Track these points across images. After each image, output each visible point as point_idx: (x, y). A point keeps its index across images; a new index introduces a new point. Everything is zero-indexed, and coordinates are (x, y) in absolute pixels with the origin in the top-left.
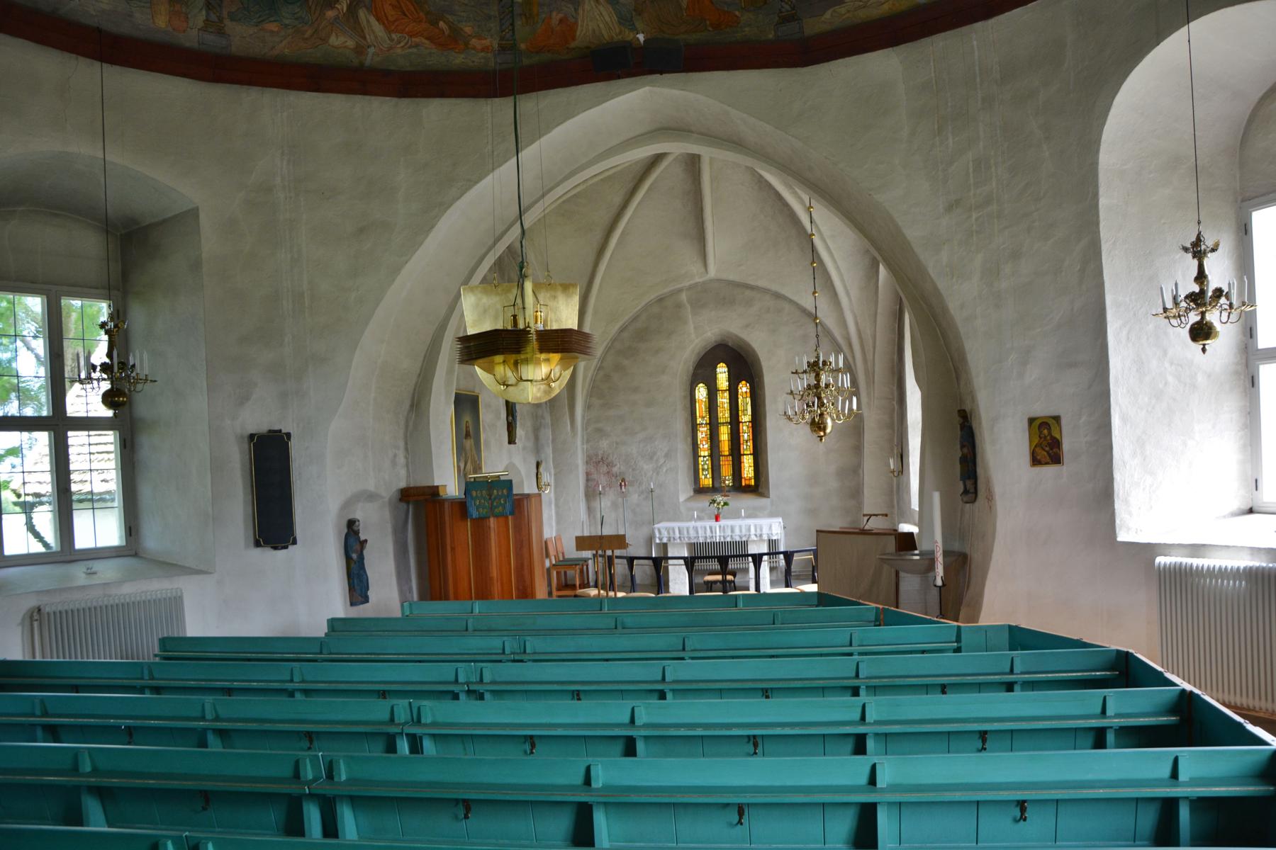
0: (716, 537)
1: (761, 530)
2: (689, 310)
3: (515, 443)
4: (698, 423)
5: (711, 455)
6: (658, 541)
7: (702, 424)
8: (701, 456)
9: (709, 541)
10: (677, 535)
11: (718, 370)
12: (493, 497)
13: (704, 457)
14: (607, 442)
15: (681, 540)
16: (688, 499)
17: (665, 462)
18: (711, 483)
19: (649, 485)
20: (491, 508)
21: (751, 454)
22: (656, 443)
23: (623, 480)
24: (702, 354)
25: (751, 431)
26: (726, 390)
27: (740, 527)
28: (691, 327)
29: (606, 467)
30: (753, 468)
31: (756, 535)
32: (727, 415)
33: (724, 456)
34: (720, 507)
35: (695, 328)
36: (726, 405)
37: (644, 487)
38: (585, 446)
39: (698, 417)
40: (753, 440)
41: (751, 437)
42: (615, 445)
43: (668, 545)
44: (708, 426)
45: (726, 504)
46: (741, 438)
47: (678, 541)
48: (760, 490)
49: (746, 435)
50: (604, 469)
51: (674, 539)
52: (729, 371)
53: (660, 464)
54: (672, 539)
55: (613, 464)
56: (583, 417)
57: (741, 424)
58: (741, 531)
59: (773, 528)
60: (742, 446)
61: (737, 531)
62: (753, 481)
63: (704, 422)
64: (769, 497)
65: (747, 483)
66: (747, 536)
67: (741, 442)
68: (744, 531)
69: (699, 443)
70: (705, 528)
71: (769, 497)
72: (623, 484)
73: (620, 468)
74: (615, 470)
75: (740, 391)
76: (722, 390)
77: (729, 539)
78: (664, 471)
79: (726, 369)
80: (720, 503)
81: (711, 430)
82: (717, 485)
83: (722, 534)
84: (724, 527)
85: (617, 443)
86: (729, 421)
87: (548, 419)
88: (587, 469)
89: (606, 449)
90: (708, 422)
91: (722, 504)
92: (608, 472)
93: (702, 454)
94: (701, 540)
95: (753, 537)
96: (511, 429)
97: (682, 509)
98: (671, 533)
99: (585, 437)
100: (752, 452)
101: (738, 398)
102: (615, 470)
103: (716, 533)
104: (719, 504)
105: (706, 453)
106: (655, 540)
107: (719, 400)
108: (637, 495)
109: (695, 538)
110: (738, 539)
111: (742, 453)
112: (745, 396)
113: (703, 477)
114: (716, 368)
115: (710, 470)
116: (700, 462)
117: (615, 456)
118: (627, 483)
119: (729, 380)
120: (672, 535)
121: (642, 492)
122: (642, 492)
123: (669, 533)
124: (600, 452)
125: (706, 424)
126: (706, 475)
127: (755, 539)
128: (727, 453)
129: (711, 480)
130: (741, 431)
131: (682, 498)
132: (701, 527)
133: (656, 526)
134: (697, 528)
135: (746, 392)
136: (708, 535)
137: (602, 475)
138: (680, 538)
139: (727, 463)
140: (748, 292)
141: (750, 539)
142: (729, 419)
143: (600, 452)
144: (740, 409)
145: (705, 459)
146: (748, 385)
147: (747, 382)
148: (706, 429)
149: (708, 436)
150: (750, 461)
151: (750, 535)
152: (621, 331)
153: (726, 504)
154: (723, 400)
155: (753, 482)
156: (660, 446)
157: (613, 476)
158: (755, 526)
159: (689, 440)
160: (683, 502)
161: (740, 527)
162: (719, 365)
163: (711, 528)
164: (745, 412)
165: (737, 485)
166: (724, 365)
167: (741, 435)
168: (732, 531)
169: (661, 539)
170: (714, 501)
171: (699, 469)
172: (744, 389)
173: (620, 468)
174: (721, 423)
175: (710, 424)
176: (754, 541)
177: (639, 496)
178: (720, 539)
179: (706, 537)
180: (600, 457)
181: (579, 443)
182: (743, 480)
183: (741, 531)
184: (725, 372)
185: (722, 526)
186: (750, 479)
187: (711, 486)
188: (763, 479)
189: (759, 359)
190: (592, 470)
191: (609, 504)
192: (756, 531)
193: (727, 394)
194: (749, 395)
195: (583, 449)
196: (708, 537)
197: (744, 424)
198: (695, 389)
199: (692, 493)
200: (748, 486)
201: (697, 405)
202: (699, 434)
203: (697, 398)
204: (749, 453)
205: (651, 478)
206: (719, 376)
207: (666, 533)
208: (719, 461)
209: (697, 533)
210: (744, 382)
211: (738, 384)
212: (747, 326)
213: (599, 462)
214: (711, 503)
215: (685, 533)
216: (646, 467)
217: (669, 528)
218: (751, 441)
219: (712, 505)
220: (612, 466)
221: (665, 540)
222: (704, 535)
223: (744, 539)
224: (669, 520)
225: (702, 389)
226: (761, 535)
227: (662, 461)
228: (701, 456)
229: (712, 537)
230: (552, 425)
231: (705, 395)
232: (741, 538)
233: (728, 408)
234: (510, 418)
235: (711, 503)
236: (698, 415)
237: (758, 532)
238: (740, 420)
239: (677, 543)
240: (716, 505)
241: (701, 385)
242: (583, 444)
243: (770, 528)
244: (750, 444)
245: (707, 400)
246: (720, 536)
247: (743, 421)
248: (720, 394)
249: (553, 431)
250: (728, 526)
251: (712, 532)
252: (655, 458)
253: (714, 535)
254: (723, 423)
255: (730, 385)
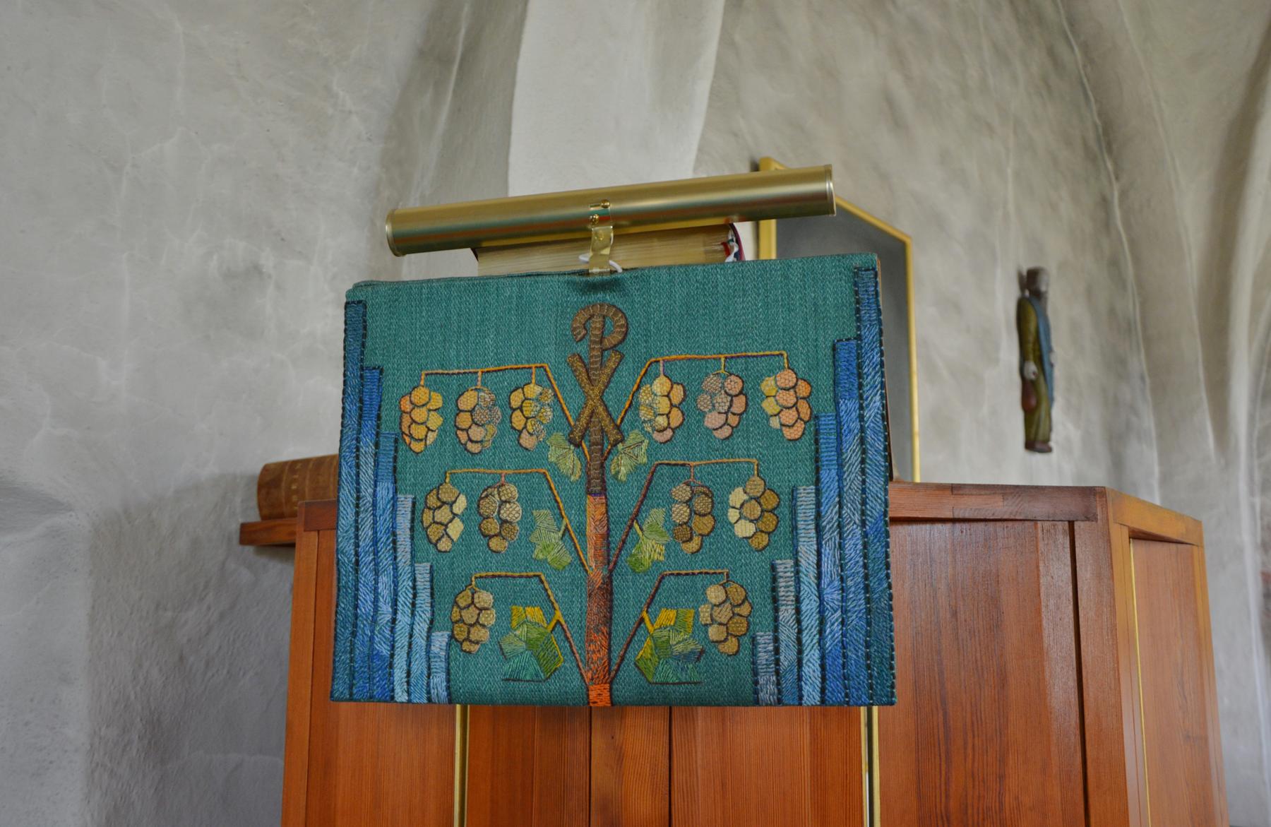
3: (1049, 450)
12: (622, 466)
20: (607, 590)
38: (1258, 501)
56: (1252, 418)
87: (1148, 421)
88: (1264, 564)
96: (1033, 402)
99: (1257, 476)
181: (1243, 487)
195: (1252, 507)
230: (1160, 437)
234: (1032, 367)
242: (1252, 493)
249: (1164, 456)
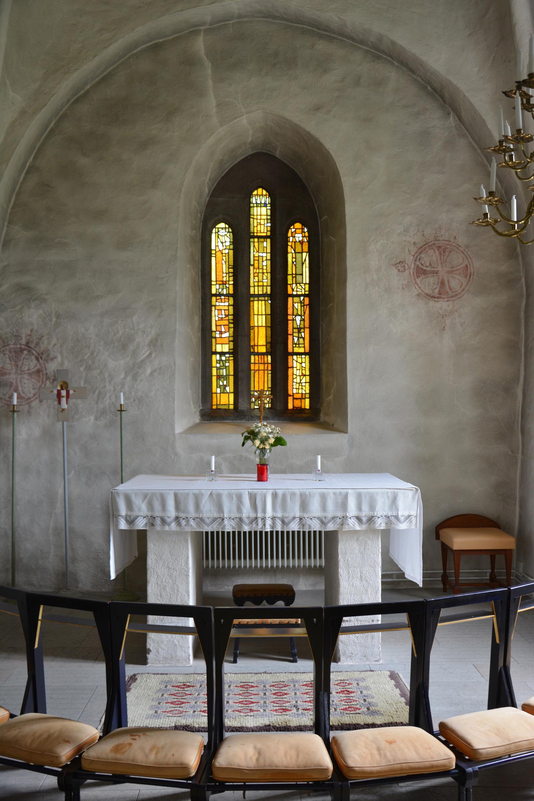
0: (264, 519)
1: (372, 507)
2: (209, 71)
4: (214, 291)
5: (234, 352)
6: (123, 525)
7: (220, 295)
8: (216, 353)
9: (246, 528)
10: (172, 512)
11: (253, 200)
13: (222, 354)
14: (41, 312)
15: (179, 524)
16: (192, 429)
17: (150, 354)
18: (232, 401)
19: (118, 398)
21: (305, 354)
22: (135, 318)
23: (65, 386)
24: (228, 166)
25: (307, 312)
26: (265, 237)
27: (324, 498)
28: (211, 102)
29: (35, 361)
30: (308, 379)
31: (359, 519)
32: (266, 280)
33: (258, 354)
34: (267, 447)
35: (218, 105)
36: (265, 263)
37: (107, 402)
39: (213, 283)
40: (310, 328)
41: (307, 324)
42: (54, 319)
43: (148, 534)
44: (231, 299)
45: (279, 441)
46: (290, 323)
47: (173, 526)
48: (323, 417)
49: (298, 318)
50: (32, 364)
51: (163, 521)
52: (272, 204)
53: (139, 360)
54: (158, 521)
55: (48, 356)
57: (290, 299)
58: (324, 508)
59: (401, 503)
60: (290, 337)
61: (315, 509)
62: (307, 401)
63: (225, 292)
64: (345, 431)
65: (297, 403)
66: (339, 521)
67: (290, 331)
68: (331, 510)
69: (214, 328)
70: (239, 498)
71: (345, 431)
72: (64, 393)
73: (62, 364)
74: (52, 367)
75: (291, 239)
76: (259, 237)
77: (294, 527)
78: (149, 371)
79: (268, 200)
80: (267, 438)
81: (235, 306)
82: (243, 406)
83: (279, 514)
84: (284, 495)
85: (58, 316)
86: (269, 292)
89: (35, 327)
90: (231, 292)
91: (272, 441)
92: (38, 371)
93: (219, 348)
94: (229, 527)
95: (353, 524)
97: (180, 447)
98: (157, 505)
100: (307, 350)
101: (287, 253)
102: (52, 367)
103: (264, 511)
104: (263, 442)
105: (226, 348)
106: (117, 524)
107: (253, 253)
108: (92, 418)
109: (215, 519)
110: (316, 526)
111: (290, 350)
112: (299, 249)
113: (219, 390)
114: (250, 195)
115: (231, 379)
116: (214, 364)
117: (54, 341)
118: (71, 392)
119: (273, 218)
120: (158, 513)
121: (103, 412)
122: (103, 412)
123: (150, 506)
124: (24, 333)
125: (228, 295)
126: (225, 386)
127: (358, 528)
128: (263, 350)
129: (232, 396)
130: (290, 311)
131: (180, 426)
132: (230, 496)
133: (121, 488)
134: (219, 496)
135: (301, 242)
136: (244, 516)
137: (26, 376)
138: (177, 518)
139: (262, 367)
140: (322, 46)
141: (346, 528)
142: (269, 288)
143: (24, 333)
144: (290, 272)
145: (223, 358)
146: (306, 230)
147: (304, 224)
148: (227, 304)
149: (231, 317)
150: (303, 365)
151: (345, 518)
152: (77, 101)
153: (279, 441)
154: (261, 254)
155: (307, 404)
156: (142, 326)
157: (48, 378)
158: (359, 497)
159: (197, 321)
160: (181, 434)
161: (324, 498)
162: (255, 193)
163: (253, 498)
164: (299, 278)
165: (279, 406)
166: (265, 192)
167: (290, 317)
168: (304, 506)
169: (131, 521)
170: (253, 435)
171: (211, 376)
172: (299, 237)
173: (62, 364)
174: (254, 296)
175: (234, 296)
176: (356, 532)
177: (96, 419)
178: (274, 525)
179: (241, 519)
180: (24, 341)
182: (290, 399)
183: (324, 508)
184: (265, 205)
185: (280, 493)
186: (302, 398)
187: (232, 407)
188: (329, 398)
189: (339, 172)
190: (8, 366)
191: (37, 432)
192: (359, 508)
193: (267, 244)
194: (306, 247)
196: (246, 521)
197: (296, 299)
198: (211, 233)
199: (197, 419)
200: (299, 411)
201: (213, 259)
202: (215, 313)
203: (213, 247)
204: (302, 350)
205: (123, 385)
206: (255, 211)
207: (144, 506)
208: (250, 363)
209: (220, 508)
210: (298, 225)
211: (289, 228)
212: (318, 108)
213: (22, 350)
214: (246, 438)
215: (191, 507)
216: (112, 364)
217: (153, 495)
218: (307, 331)
219: (249, 442)
220: (47, 361)
221: (141, 524)
222: (235, 514)
223: (331, 527)
224: (155, 471)
225: (222, 232)
226: (371, 520)
227: (144, 353)
228: (216, 353)
229: (256, 518)
231: (228, 244)
232: (323, 523)
233: (269, 270)
235: (246, 438)
236: (213, 278)
237: (365, 512)
238: (290, 291)
239: (171, 533)
240: (257, 442)
241: (222, 225)
243: (394, 501)
244: (306, 334)
245: (231, 252)
246: (273, 518)
247: (295, 293)
248: (254, 244)
250: (293, 494)
251: (254, 506)
252: (131, 348)
253: (260, 515)
254: (259, 296)
255: (273, 229)
